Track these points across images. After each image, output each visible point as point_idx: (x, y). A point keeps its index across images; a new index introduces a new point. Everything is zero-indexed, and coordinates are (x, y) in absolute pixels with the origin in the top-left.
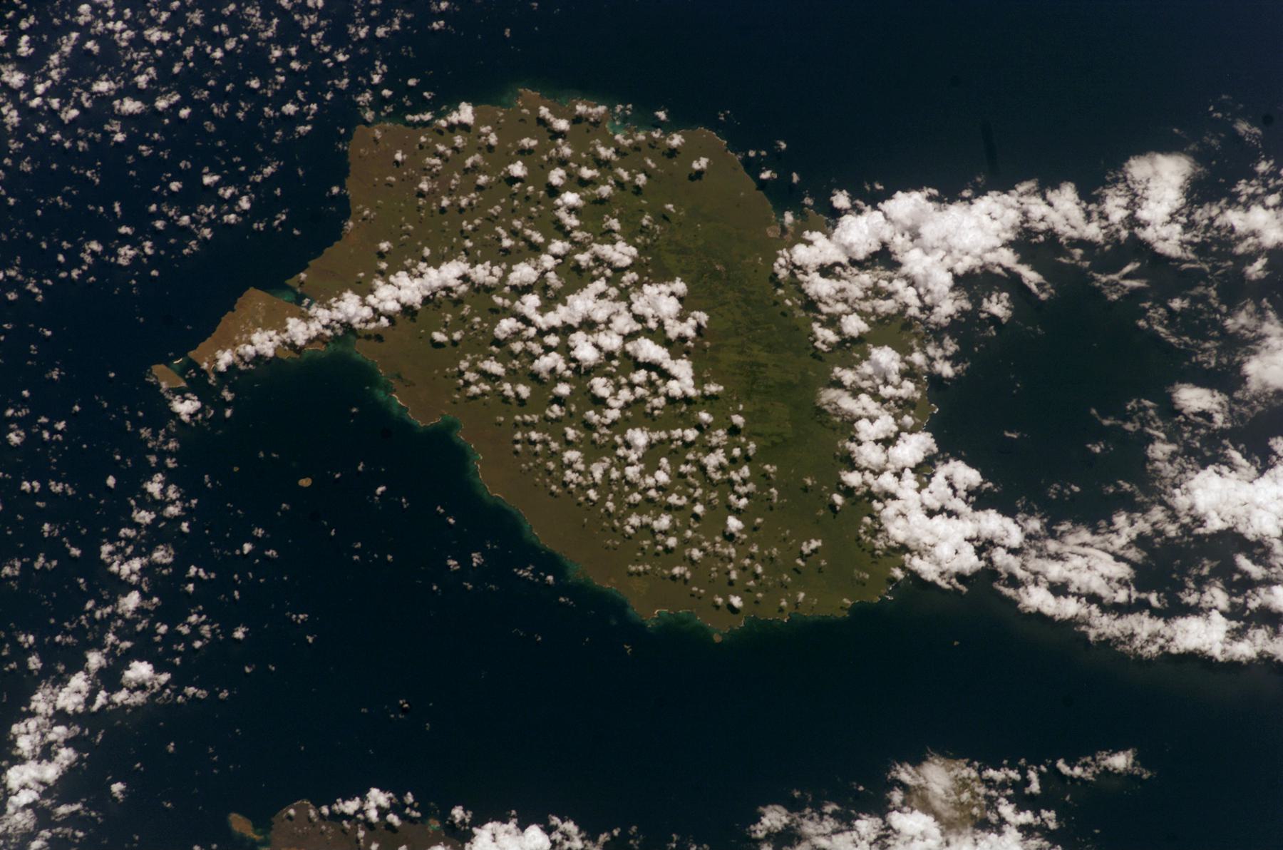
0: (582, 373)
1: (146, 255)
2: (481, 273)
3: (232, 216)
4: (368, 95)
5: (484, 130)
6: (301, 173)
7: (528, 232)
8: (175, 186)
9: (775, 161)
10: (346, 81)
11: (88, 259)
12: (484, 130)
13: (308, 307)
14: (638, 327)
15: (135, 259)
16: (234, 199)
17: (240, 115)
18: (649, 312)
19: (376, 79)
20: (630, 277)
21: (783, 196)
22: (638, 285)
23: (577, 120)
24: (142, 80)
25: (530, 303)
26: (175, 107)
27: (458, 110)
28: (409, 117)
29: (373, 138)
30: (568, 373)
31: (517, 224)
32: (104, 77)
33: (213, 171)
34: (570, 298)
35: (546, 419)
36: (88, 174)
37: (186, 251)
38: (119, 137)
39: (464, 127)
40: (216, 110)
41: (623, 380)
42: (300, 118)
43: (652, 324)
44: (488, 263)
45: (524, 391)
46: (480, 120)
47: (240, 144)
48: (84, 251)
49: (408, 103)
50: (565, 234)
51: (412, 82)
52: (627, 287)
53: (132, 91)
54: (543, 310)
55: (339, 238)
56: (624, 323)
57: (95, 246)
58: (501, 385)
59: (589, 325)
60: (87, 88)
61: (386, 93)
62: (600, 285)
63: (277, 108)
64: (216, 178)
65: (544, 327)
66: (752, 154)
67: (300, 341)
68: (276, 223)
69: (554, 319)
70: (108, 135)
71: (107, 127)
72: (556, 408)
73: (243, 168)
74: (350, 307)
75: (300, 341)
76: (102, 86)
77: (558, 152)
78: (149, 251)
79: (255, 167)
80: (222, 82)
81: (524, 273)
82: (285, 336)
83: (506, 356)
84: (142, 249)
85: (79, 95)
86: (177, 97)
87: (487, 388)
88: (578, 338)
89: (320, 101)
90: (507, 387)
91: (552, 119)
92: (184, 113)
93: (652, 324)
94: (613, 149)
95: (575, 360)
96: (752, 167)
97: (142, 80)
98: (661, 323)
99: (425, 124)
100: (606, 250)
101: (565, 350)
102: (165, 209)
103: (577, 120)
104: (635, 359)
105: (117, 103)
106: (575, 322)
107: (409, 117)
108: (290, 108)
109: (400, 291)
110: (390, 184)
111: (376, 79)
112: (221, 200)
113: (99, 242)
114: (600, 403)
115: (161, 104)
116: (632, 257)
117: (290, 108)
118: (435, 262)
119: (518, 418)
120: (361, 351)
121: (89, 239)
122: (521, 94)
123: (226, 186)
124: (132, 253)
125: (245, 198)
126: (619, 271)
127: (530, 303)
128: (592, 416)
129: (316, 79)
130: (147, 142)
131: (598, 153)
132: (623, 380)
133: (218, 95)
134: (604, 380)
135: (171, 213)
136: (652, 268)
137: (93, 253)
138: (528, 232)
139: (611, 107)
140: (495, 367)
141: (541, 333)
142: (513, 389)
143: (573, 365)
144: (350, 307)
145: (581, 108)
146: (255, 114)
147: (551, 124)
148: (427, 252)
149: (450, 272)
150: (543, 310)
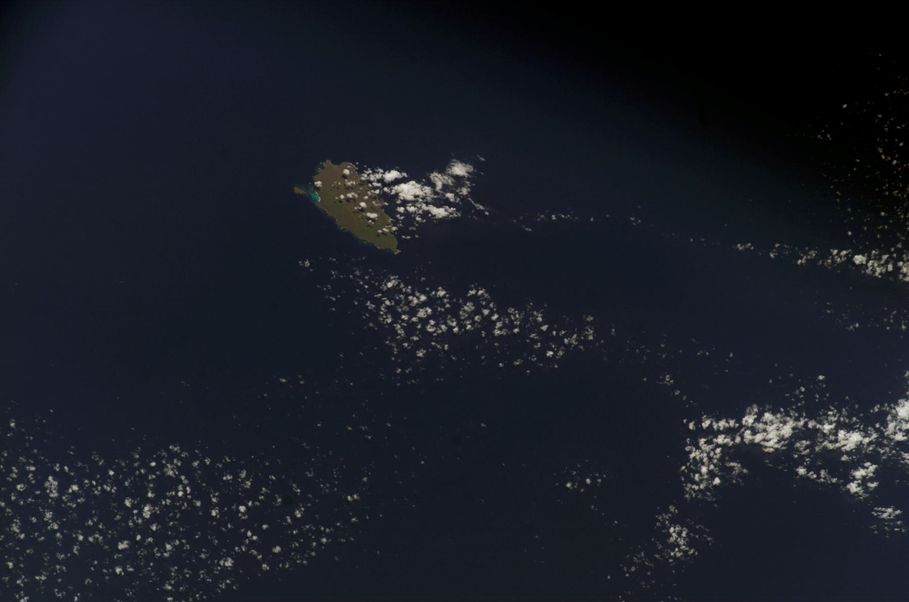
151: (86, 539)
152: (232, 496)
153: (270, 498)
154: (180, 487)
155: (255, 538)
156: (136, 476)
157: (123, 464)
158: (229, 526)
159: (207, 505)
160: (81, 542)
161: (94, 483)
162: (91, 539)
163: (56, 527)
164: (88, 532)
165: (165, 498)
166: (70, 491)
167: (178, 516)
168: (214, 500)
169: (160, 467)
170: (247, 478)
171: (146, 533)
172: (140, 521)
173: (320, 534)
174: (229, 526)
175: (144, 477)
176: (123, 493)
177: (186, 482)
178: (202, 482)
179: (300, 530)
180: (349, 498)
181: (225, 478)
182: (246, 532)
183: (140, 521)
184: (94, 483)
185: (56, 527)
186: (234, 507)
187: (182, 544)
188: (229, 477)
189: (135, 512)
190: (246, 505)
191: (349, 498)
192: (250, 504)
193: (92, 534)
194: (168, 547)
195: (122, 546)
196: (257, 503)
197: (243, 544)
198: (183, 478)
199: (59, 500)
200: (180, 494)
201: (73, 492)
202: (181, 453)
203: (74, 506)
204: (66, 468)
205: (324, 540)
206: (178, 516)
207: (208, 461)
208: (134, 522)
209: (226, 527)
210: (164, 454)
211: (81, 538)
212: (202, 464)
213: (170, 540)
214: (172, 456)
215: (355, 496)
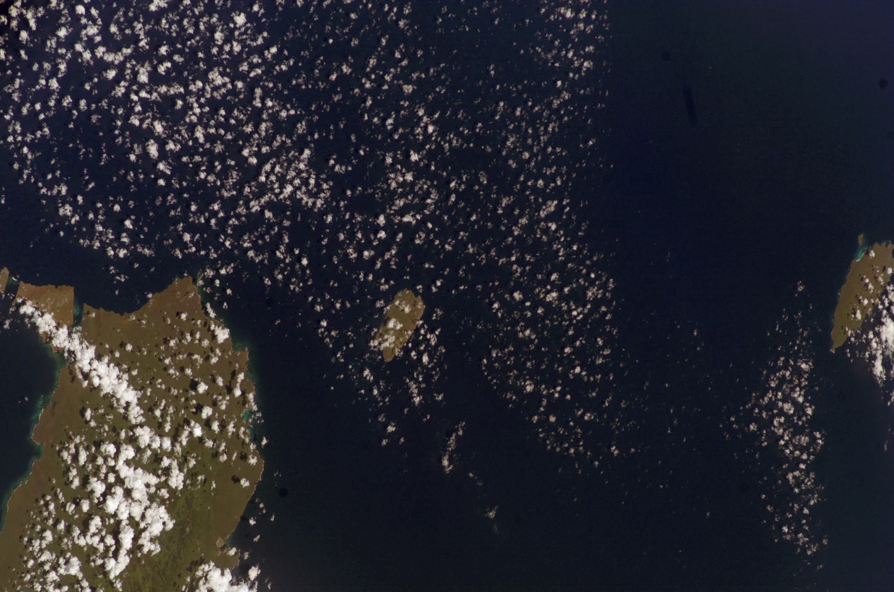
0: (99, 508)
1: (70, 221)
2: (136, 414)
3: (112, 253)
4: (212, 274)
5: (218, 351)
6: (152, 270)
7: (169, 419)
8: (117, 208)
9: (262, 520)
10: (215, 256)
11: (55, 192)
12: (218, 351)
13: (77, 331)
14: (137, 519)
15: (66, 217)
16: (123, 245)
17: (172, 213)
18: (149, 520)
19: (223, 272)
20: (164, 493)
21: (242, 537)
22: (163, 502)
23: (244, 399)
24: (171, 146)
25: (129, 452)
26: (163, 175)
27: (223, 328)
28: (208, 305)
29: (187, 289)
30: (96, 501)
31: (171, 410)
32: (164, 124)
33: (134, 223)
34: (140, 471)
35: (64, 506)
36: (105, 155)
37: (81, 241)
38: (133, 157)
39: (214, 337)
40: (169, 198)
41: (104, 533)
42: (184, 246)
43: (142, 525)
44: (142, 412)
45: (76, 483)
46: (223, 347)
47: (157, 225)
48: (59, 186)
49: (216, 298)
50: (175, 437)
51: (229, 291)
52: (159, 497)
53: (161, 143)
54: (128, 463)
55: (122, 314)
56: (137, 511)
57: (64, 190)
58: (73, 468)
59: (128, 493)
60: (154, 119)
61: (217, 282)
62: (153, 480)
63: (185, 230)
64: (131, 227)
65: (117, 468)
66: (262, 506)
67: (56, 343)
68: (118, 278)
69: (125, 471)
70: (131, 150)
71: (136, 146)
72: (73, 506)
73: (142, 237)
74: (85, 356)
75: (56, 343)
76: (159, 128)
77: (221, 400)
78: (73, 221)
79: (146, 243)
80: (186, 190)
81: (145, 435)
82: (54, 331)
83: (92, 459)
84: (72, 216)
85: (149, 117)
86: (169, 172)
87: (69, 462)
88: (119, 491)
89: (198, 251)
90: (74, 472)
91: (238, 385)
92: (161, 182)
93: (142, 525)
94: (234, 430)
95: (105, 501)
96: (251, 509)
97: (171, 146)
98: (145, 529)
99: (207, 314)
100: (175, 472)
101: (108, 492)
102: (101, 212)
103: (244, 399)
104: (119, 533)
105: (152, 141)
106: (128, 485)
107: (208, 305)
108: (187, 237)
109: (108, 378)
110: (164, 320)
111: (223, 272)
112: (118, 238)
113: (67, 191)
114: (84, 532)
115: (161, 166)
116: (176, 488)
117: (187, 237)
118: (132, 382)
119: (59, 490)
120: (61, 375)
121: (67, 184)
122: (244, 350)
123: (129, 236)
124: (69, 214)
125: (125, 251)
126: (165, 485)
127: (129, 452)
128: (77, 532)
129: (208, 237)
130: (136, 175)
131: (229, 424)
132: (104, 533)
133: (178, 194)
134: (100, 524)
135: (100, 217)
136: (174, 503)
137: (59, 192)
138: (169, 419)
139: (258, 411)
140: (83, 457)
141: (112, 469)
142: (74, 477)
143: (101, 499)
144: (85, 356)
145: (251, 396)
146: (175, 221)
147: (235, 386)
148: (135, 373)
149: (128, 395)
150: (128, 463)
151: (514, 262)
152: (584, 356)
153: (592, 386)
154: (580, 309)
155: (557, 395)
156: (578, 268)
157: (585, 252)
158: (560, 369)
159: (571, 341)
160: (510, 260)
161: (562, 239)
162: (515, 267)
163: (516, 233)
164: (521, 262)
165: (568, 304)
166: (550, 225)
167: (556, 323)
168: (578, 343)
169: (592, 283)
170: (604, 357)
171: (533, 308)
172: (542, 296)
173: (575, 445)
174: (560, 369)
175: (578, 275)
176: (560, 268)
177: (586, 311)
178: (590, 324)
179: (574, 427)
180: (614, 448)
181: (599, 339)
182: (559, 385)
183: (542, 296)
184: (562, 239)
185: (516, 233)
186: (577, 362)
187: (532, 341)
188: (600, 343)
189: (549, 287)
190: (581, 371)
191: (614, 448)
192: (584, 373)
193: (519, 265)
194: (528, 332)
195: (517, 296)
196: (586, 379)
197: (549, 390)
198: (589, 306)
199: (540, 220)
200: (575, 313)
201: (549, 228)
202: (609, 291)
203: (538, 236)
204: (568, 209)
205: (572, 451)
206: (556, 323)
207: (608, 317)
208: (540, 291)
209: (558, 367)
210: (604, 279)
211: (513, 259)
212: (605, 314)
213: (534, 330)
214: (604, 286)
215: (616, 452)
